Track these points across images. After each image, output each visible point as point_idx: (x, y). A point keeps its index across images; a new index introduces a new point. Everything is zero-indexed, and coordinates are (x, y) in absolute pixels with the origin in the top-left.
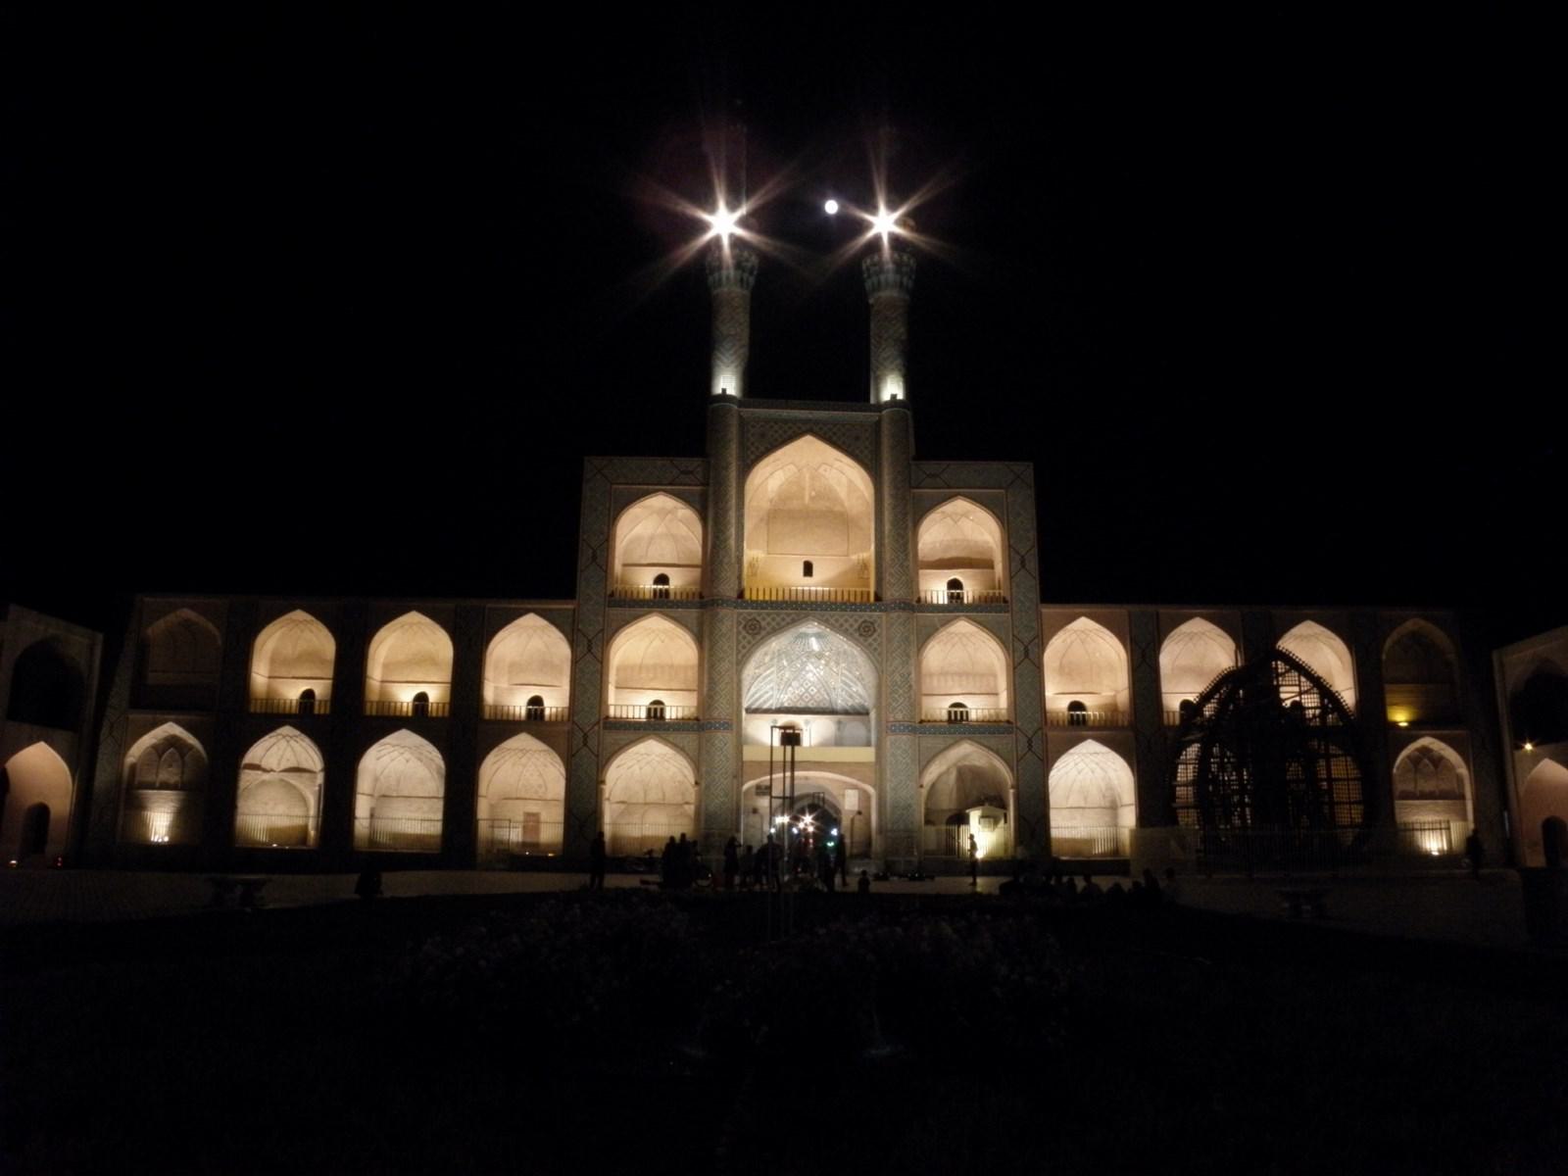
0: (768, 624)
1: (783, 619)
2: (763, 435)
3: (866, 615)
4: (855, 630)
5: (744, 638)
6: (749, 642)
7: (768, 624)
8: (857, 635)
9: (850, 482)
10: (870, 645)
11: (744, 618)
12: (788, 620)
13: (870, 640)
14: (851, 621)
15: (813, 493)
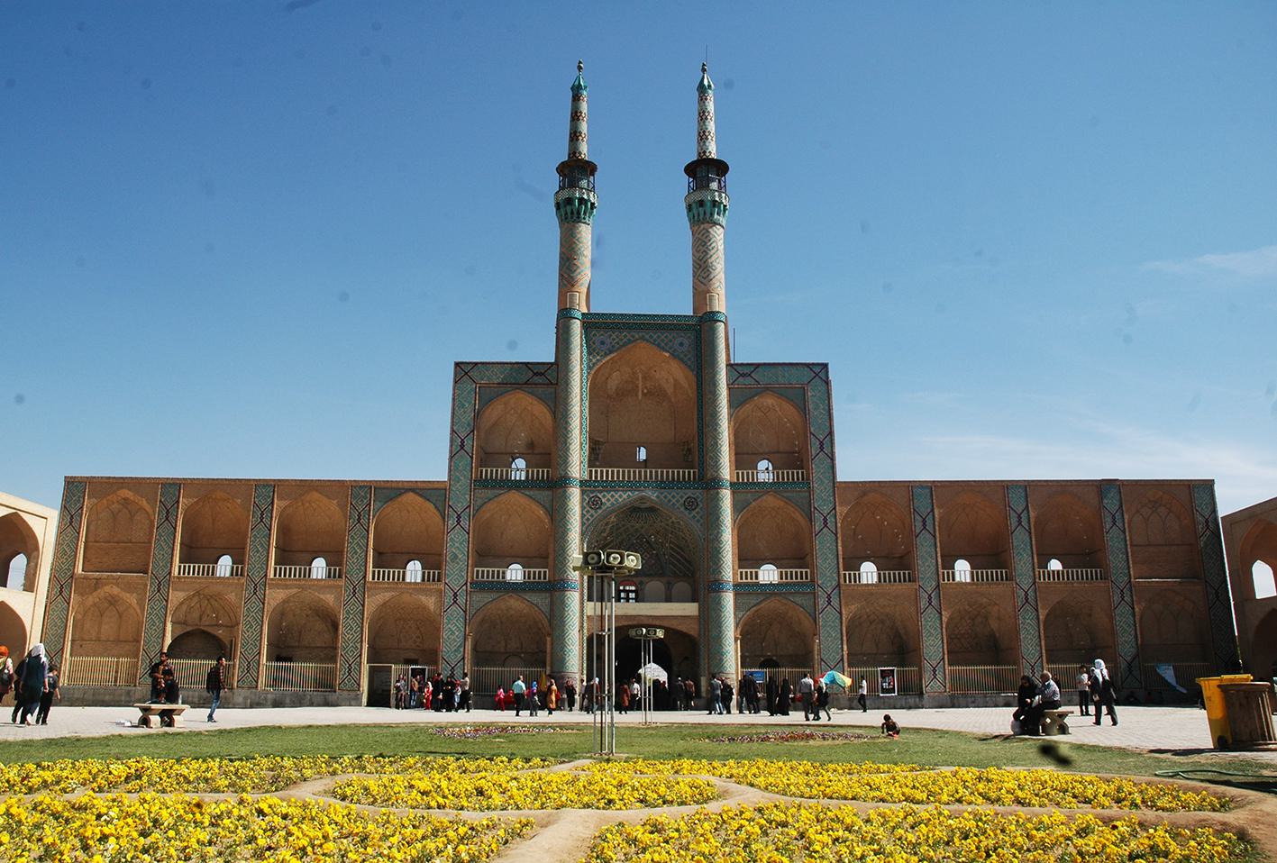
0: (608, 500)
1: (620, 496)
2: (603, 343)
3: (689, 493)
4: (681, 505)
5: (588, 512)
6: (592, 516)
7: (608, 500)
8: (682, 509)
9: (675, 380)
10: (694, 517)
11: (588, 496)
12: (625, 496)
13: (694, 513)
14: (678, 497)
15: (645, 391)
